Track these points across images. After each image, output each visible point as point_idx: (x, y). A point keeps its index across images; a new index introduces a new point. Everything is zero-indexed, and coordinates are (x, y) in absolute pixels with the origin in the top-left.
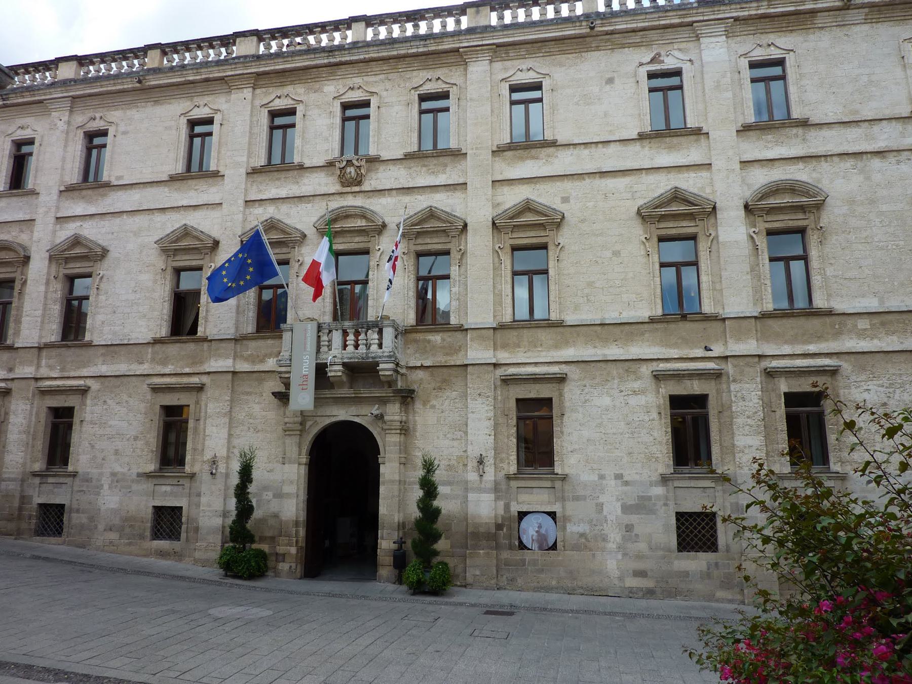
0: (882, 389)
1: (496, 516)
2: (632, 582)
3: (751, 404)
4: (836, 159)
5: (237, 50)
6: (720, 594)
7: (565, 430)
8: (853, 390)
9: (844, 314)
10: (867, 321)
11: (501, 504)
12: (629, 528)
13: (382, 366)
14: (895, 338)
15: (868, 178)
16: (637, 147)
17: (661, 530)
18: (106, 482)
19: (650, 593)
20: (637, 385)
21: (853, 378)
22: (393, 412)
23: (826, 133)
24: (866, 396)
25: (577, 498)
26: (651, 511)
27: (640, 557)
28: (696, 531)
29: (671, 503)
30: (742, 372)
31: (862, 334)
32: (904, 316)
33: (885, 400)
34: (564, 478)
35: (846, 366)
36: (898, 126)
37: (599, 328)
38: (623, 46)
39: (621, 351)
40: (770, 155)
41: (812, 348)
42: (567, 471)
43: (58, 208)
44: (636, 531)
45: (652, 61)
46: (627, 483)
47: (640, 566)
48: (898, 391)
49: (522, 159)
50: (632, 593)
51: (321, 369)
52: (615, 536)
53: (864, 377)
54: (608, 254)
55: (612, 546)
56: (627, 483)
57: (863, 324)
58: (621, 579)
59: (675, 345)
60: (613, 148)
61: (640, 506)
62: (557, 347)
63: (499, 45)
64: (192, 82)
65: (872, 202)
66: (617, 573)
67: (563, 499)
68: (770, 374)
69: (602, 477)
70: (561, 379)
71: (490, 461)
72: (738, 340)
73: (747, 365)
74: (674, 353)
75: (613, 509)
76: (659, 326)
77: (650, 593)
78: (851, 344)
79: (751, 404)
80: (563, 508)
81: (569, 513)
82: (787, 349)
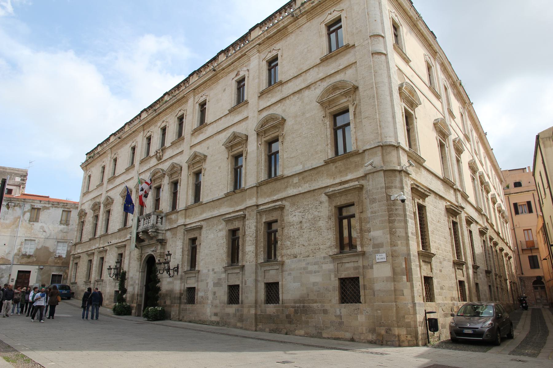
0: (300, 214)
1: (180, 290)
2: (214, 319)
3: (252, 230)
4: (292, 97)
5: (142, 118)
6: (239, 324)
7: (201, 251)
8: (290, 217)
9: (288, 177)
10: (297, 178)
11: (183, 284)
12: (215, 293)
13: (150, 230)
14: (307, 185)
15: (303, 102)
16: (228, 117)
17: (223, 294)
18: (108, 283)
19: (218, 324)
20: (220, 227)
21: (290, 210)
22: (159, 249)
23: (290, 84)
24: (294, 218)
25: (202, 281)
26: (221, 285)
27: (216, 306)
28: (234, 294)
29: (227, 282)
30: (250, 215)
31: (295, 186)
32: (312, 172)
33: (301, 219)
34: (199, 271)
35: (286, 203)
36: (316, 69)
37: (212, 203)
38: (229, 73)
39: (218, 212)
40: (268, 104)
41: (275, 198)
42: (200, 269)
43: (107, 188)
44: (217, 295)
45: (236, 75)
46: (215, 273)
47: (215, 311)
48: (307, 214)
49: (199, 134)
50: (212, 323)
51: (138, 234)
52: (210, 297)
53: (294, 209)
54: (217, 168)
55: (209, 302)
56: (215, 273)
57: (296, 180)
58: (210, 316)
59: (231, 207)
60: (223, 119)
61: (217, 284)
62: (201, 214)
63: (194, 89)
64: (131, 134)
65: (303, 114)
66: (209, 314)
67: (198, 281)
68: (260, 213)
69: (209, 271)
70: (200, 228)
71: (180, 266)
72: (250, 199)
73: (252, 211)
74: (231, 210)
75: (211, 285)
76: (229, 198)
77: (218, 324)
78: (292, 191)
79: (252, 230)
80: (198, 285)
81: (199, 288)
82: (266, 201)
